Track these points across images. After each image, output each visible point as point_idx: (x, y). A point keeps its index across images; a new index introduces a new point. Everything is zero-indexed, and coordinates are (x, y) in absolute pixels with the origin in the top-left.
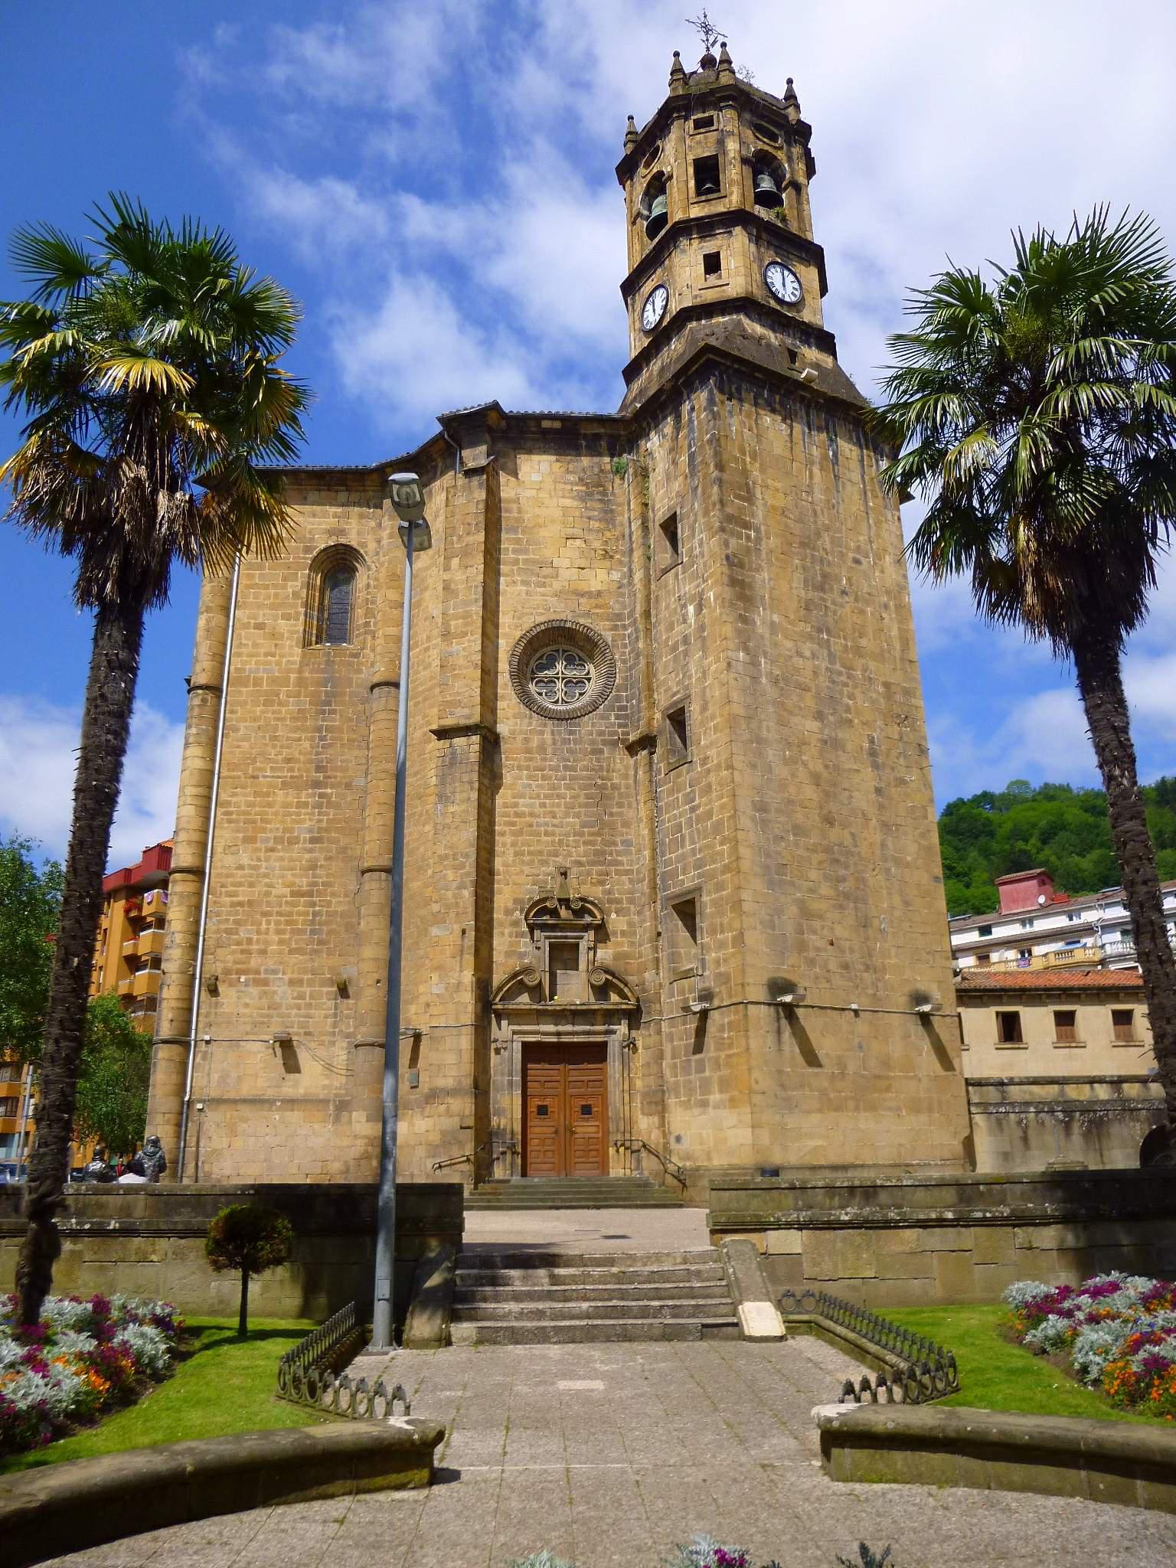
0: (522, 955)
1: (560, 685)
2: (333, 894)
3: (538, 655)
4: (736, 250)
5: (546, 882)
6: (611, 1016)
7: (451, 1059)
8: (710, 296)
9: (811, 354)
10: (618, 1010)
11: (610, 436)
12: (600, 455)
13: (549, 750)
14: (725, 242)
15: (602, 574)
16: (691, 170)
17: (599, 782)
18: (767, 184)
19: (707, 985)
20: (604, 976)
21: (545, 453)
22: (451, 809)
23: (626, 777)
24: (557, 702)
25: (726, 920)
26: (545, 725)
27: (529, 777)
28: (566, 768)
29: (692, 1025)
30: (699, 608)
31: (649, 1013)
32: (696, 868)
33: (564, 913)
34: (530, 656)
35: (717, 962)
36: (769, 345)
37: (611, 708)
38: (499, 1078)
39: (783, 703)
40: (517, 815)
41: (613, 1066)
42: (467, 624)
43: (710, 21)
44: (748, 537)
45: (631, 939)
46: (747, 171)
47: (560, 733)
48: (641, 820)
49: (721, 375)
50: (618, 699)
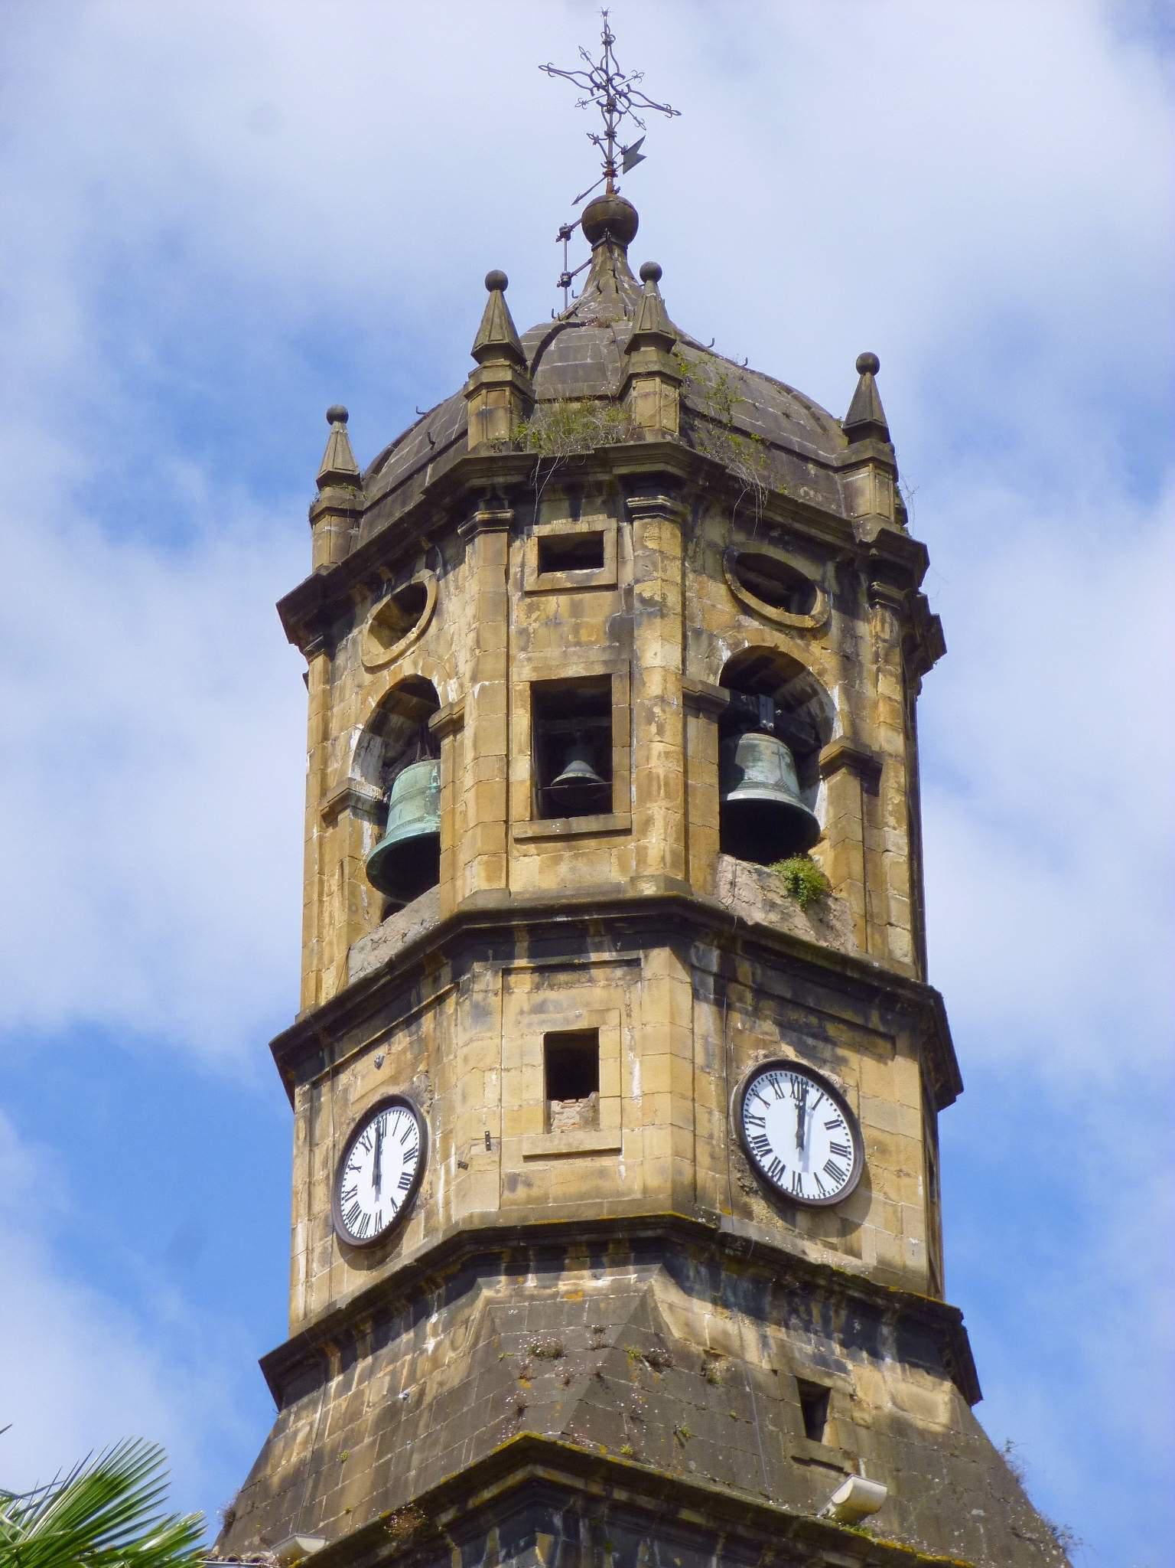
4: (649, 1015)
8: (560, 1191)
9: (882, 1386)
14: (617, 995)
16: (522, 720)
18: (766, 775)
36: (737, 1378)
43: (626, 58)
46: (703, 733)
49: (572, 1531)
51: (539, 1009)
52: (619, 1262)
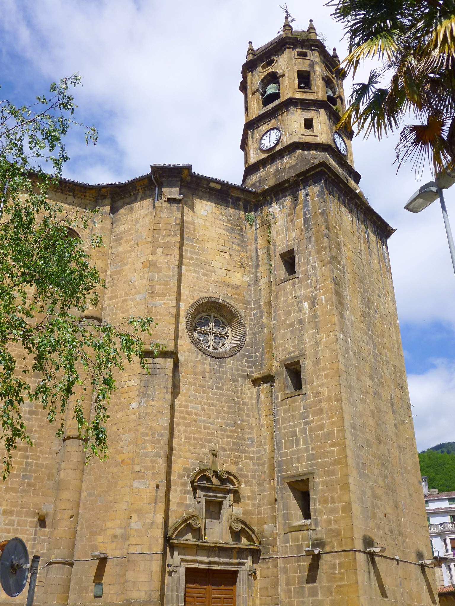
0: (188, 506)
1: (211, 336)
2: (42, 452)
3: (199, 316)
4: (321, 119)
5: (204, 459)
6: (242, 553)
7: (144, 577)
8: (308, 139)
10: (247, 549)
11: (246, 200)
12: (239, 209)
13: (208, 375)
14: (315, 115)
15: (239, 276)
16: (296, 75)
17: (236, 399)
19: (319, 536)
20: (241, 526)
21: (209, 200)
22: (152, 403)
23: (251, 398)
24: (209, 346)
25: (336, 495)
26: (206, 360)
27: (196, 390)
28: (217, 388)
29: (306, 563)
30: (313, 304)
31: (267, 553)
32: (308, 460)
33: (215, 481)
34: (196, 316)
35: (329, 522)
37: (243, 355)
38: (170, 593)
39: (358, 367)
40: (187, 413)
41: (241, 586)
42: (166, 289)
44: (340, 270)
45: (257, 501)
47: (214, 366)
48: (262, 426)
50: (247, 351)
51: (303, 114)
52: (320, 151)
